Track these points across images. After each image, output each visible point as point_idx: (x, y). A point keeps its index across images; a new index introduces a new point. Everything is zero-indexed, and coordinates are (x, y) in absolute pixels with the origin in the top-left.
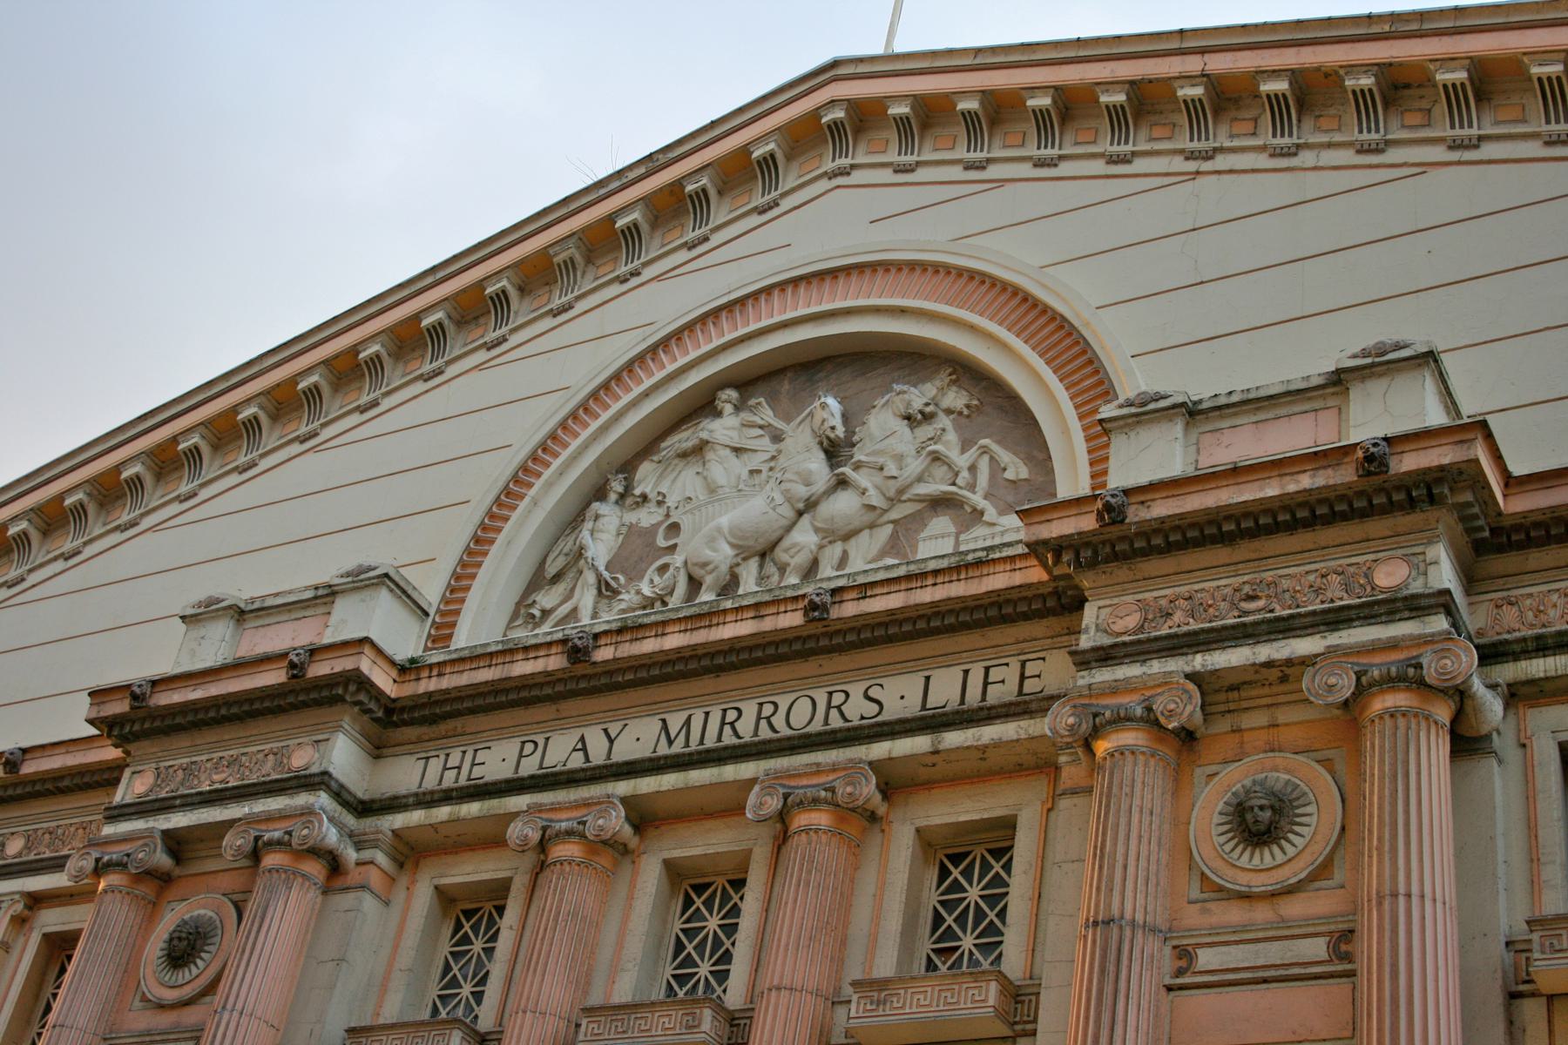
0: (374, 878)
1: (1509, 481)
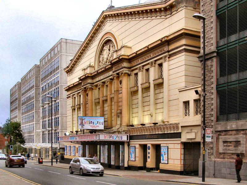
0: (95, 89)
1: (128, 56)
